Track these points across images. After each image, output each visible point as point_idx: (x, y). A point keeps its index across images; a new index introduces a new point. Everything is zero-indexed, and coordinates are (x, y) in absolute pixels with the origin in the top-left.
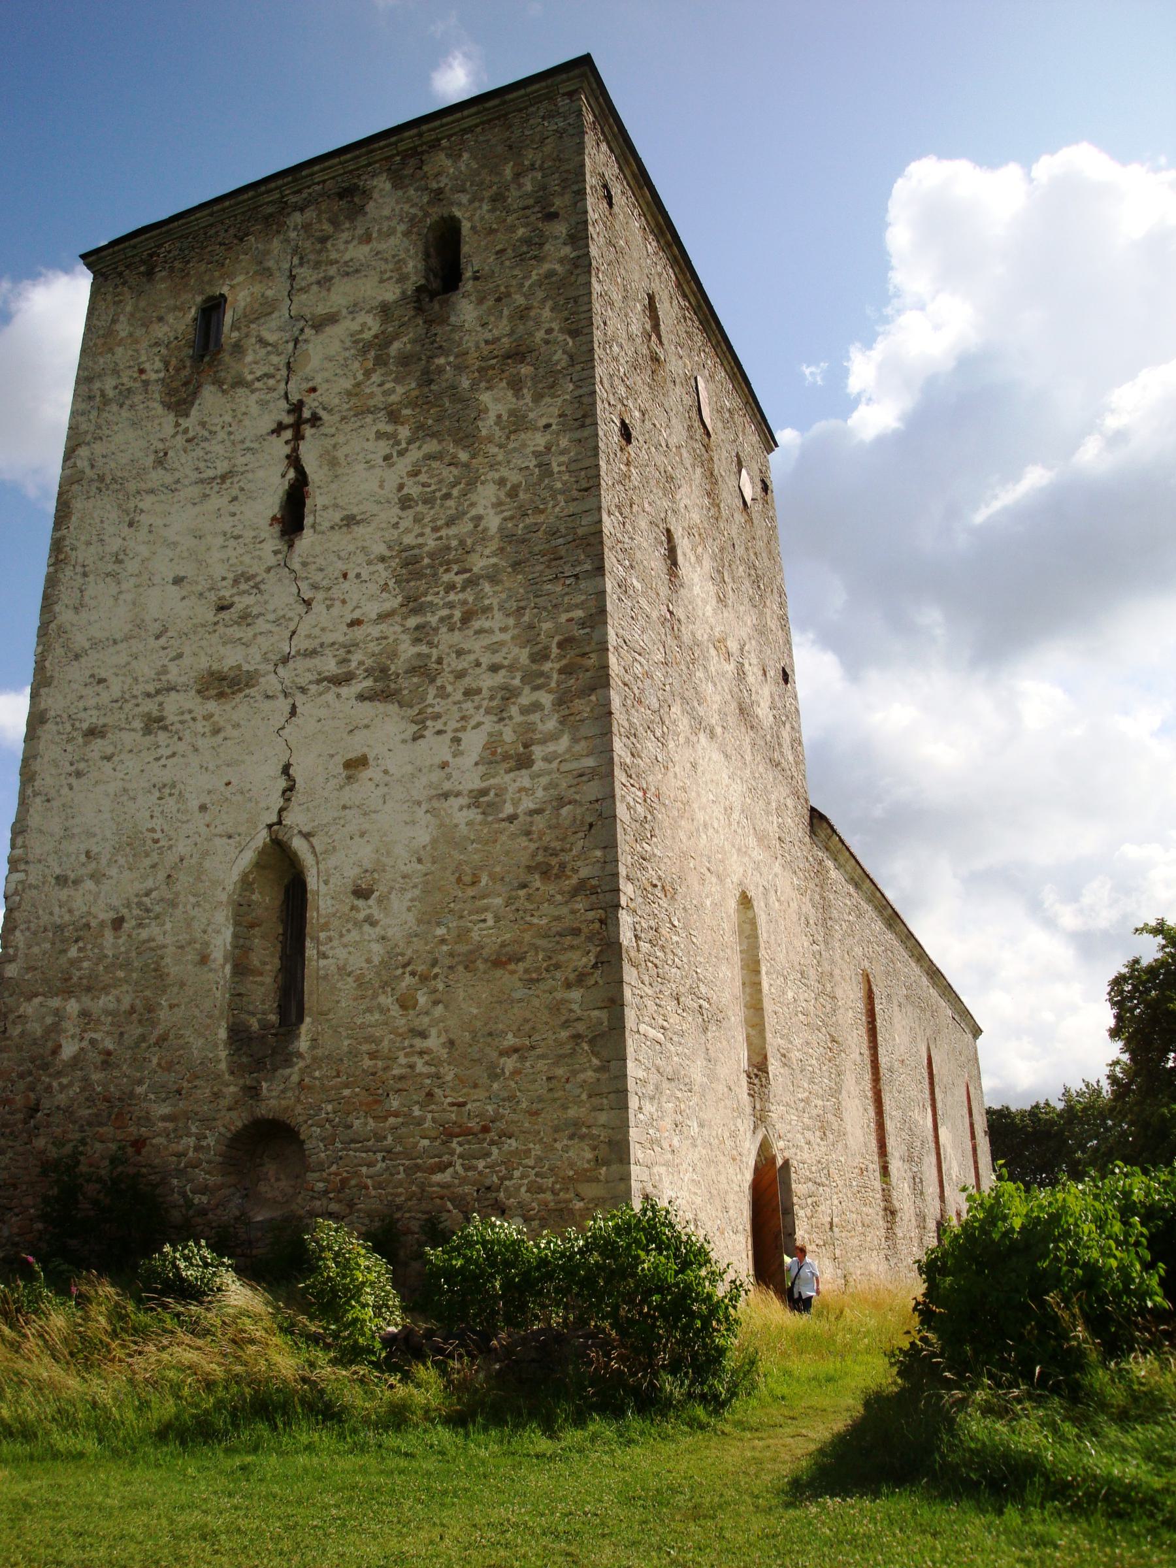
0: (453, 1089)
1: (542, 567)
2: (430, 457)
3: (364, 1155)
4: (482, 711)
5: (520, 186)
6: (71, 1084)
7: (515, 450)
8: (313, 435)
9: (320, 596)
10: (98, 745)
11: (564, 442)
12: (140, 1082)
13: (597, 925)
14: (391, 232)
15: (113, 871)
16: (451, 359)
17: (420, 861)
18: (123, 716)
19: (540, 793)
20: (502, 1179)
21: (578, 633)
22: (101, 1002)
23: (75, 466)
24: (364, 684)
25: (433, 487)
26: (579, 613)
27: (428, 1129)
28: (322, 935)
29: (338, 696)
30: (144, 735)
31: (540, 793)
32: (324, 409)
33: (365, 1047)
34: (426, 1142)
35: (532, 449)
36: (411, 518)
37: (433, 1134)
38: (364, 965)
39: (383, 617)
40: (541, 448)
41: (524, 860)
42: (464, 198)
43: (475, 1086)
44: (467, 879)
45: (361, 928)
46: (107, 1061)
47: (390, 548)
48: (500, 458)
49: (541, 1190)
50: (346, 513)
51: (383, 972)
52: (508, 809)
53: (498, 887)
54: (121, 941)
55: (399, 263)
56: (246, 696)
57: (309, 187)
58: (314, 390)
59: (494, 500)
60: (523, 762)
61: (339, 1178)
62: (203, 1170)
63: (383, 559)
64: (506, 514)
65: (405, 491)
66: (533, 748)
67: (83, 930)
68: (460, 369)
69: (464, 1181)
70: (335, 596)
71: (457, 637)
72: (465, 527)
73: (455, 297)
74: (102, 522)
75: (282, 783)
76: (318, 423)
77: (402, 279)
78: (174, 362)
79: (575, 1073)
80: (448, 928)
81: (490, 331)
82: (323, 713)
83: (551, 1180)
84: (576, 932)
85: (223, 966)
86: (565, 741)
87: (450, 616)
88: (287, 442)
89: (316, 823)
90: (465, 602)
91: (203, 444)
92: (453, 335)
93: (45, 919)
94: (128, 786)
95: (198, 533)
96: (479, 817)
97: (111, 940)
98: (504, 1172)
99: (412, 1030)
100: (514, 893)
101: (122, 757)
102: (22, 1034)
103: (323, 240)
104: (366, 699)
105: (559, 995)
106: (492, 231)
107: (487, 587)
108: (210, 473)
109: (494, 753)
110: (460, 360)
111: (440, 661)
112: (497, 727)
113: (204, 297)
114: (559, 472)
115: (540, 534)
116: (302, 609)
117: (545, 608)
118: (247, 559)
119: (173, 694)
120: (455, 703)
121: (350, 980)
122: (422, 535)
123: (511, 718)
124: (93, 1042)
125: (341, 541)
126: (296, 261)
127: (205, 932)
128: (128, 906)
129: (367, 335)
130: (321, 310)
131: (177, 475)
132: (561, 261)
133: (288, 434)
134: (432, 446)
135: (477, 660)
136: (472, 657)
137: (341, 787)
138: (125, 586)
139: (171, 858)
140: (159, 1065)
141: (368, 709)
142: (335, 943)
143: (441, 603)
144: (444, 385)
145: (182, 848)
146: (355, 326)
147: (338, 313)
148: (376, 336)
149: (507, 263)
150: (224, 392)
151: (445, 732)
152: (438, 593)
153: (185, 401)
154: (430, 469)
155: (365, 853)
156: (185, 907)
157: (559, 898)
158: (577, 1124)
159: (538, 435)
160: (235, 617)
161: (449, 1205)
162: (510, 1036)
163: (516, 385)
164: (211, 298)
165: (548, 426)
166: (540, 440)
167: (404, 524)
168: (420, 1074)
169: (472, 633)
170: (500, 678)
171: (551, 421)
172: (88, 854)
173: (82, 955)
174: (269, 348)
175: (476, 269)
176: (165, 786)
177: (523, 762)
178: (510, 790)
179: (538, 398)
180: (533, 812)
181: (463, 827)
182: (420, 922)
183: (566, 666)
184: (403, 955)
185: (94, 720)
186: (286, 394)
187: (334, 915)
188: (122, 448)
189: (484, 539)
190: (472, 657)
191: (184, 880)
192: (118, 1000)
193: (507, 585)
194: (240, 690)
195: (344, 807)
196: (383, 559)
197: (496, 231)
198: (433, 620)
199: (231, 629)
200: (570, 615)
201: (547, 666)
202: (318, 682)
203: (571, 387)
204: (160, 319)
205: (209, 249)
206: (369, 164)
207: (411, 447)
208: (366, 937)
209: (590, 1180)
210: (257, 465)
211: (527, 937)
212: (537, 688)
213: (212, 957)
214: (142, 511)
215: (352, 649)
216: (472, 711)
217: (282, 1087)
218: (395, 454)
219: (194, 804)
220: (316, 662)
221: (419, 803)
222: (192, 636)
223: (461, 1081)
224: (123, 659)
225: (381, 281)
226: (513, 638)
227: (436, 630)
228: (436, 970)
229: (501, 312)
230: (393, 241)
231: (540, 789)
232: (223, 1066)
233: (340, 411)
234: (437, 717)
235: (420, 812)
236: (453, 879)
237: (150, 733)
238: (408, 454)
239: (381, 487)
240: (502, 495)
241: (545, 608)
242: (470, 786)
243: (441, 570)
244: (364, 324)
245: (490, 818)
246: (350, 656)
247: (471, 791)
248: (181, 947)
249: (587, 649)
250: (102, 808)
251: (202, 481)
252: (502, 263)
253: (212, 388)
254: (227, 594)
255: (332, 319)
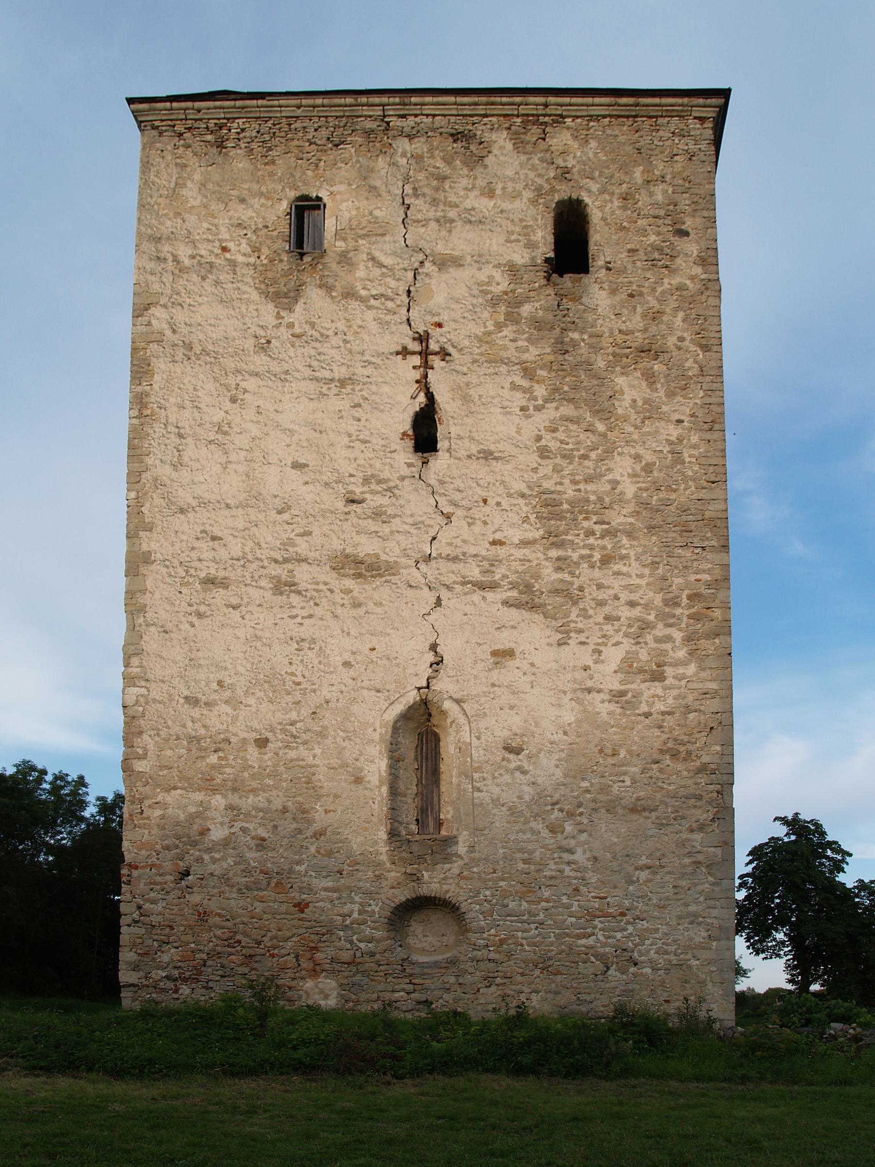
1: (674, 535)
3: (520, 925)
4: (621, 633)
5: (651, 194)
6: (224, 858)
7: (649, 433)
8: (442, 368)
9: (460, 513)
10: (219, 596)
11: (695, 439)
12: (299, 863)
13: (715, 795)
14: (516, 196)
15: (252, 701)
16: (586, 337)
17: (565, 733)
18: (247, 574)
19: (670, 701)
20: (636, 945)
21: (704, 591)
22: (250, 801)
23: (149, 324)
25: (571, 446)
26: (706, 577)
27: (575, 911)
29: (484, 598)
30: (274, 594)
31: (670, 701)
32: (454, 347)
34: (573, 919)
35: (665, 437)
36: (551, 468)
37: (579, 915)
38: (516, 800)
39: (525, 543)
40: (673, 438)
41: (657, 745)
42: (595, 187)
43: (615, 887)
44: (609, 752)
45: (512, 773)
46: (261, 844)
47: (529, 487)
48: (635, 437)
49: (666, 953)
50: (482, 447)
52: (644, 708)
53: (635, 760)
54: (266, 757)
55: (527, 231)
56: (386, 581)
57: (416, 116)
58: (440, 325)
59: (630, 471)
61: (497, 938)
62: (368, 926)
63: (523, 496)
64: (640, 485)
65: (543, 442)
66: (665, 668)
67: (221, 744)
68: (595, 348)
69: (605, 945)
70: (477, 516)
71: (597, 573)
72: (603, 487)
73: (586, 279)
74: (195, 389)
75: (431, 657)
76: (448, 358)
77: (531, 245)
78: (265, 251)
79: (696, 885)
80: (592, 784)
81: (624, 322)
82: (469, 609)
83: (674, 947)
84: (699, 798)
85: (380, 787)
86: (691, 669)
87: (591, 556)
88: (414, 367)
89: (465, 693)
90: (604, 548)
91: (314, 344)
92: (585, 315)
93: (176, 729)
94: (259, 633)
95: (317, 428)
96: (619, 711)
97: (256, 754)
98: (638, 940)
99: (560, 848)
100: (648, 766)
101: (249, 608)
102: (162, 817)
103: (442, 178)
104: (511, 606)
106: (622, 228)
107: (625, 541)
108: (327, 374)
109: (631, 666)
110: (594, 340)
111: (581, 589)
112: (634, 648)
113: (298, 194)
114: (690, 462)
115: (673, 508)
116: (442, 520)
117: (676, 567)
118: (378, 464)
119: (304, 566)
120: (596, 624)
121: (504, 809)
122: (561, 484)
123: (646, 643)
124: (244, 830)
125: (480, 470)
126: (408, 189)
127: (357, 760)
128: (272, 730)
129: (497, 290)
130: (440, 248)
131: (286, 367)
132: (692, 278)
134: (568, 410)
136: (611, 592)
137: (490, 670)
138: (233, 457)
139: (314, 700)
140: (318, 852)
141: (514, 615)
142: (489, 782)
143: (582, 544)
144: (579, 359)
145: (325, 693)
146: (482, 276)
147: (461, 258)
148: (506, 293)
149: (639, 264)
150: (332, 297)
151: (588, 644)
152: (578, 535)
153: (286, 295)
154: (567, 430)
155: (516, 722)
156: (335, 738)
157: (685, 773)
158: (696, 915)
159: (671, 427)
160: (369, 512)
161: (593, 959)
163: (650, 378)
164: (305, 198)
165: (680, 421)
166: (674, 432)
167: (542, 472)
168: (569, 877)
169: (611, 573)
170: (637, 612)
171: (682, 418)
172: (220, 683)
173: (223, 763)
174: (384, 270)
175: (608, 259)
176: (303, 640)
177: (657, 677)
178: (645, 695)
179: (671, 394)
180: (663, 713)
182: (566, 776)
183: (695, 614)
184: (551, 797)
185: (213, 572)
186: (408, 320)
187: (487, 762)
188: (212, 321)
189: (621, 500)
190: (611, 592)
191: (329, 719)
192: (269, 802)
193: (642, 542)
194: (381, 576)
195: (493, 685)
196: (523, 496)
197: (628, 229)
198: (575, 556)
199: (366, 522)
200: (699, 577)
201: (678, 611)
202: (463, 584)
203: (701, 394)
204: (243, 201)
205: (295, 143)
206: (486, 116)
207: (547, 405)
208: (518, 781)
210: (380, 380)
211: (659, 796)
212: (671, 625)
213: (367, 779)
214: (245, 391)
215: (496, 563)
216: (611, 632)
217: (442, 876)
218: (531, 408)
219: (337, 660)
220: (460, 566)
221: (565, 693)
222: (321, 519)
223: (603, 883)
224: (241, 523)
226: (648, 584)
227: (577, 564)
228: (581, 810)
229: (635, 308)
230: (517, 204)
231: (671, 698)
232: (384, 858)
233: (471, 354)
234: (581, 631)
235: (566, 699)
236: (596, 750)
237: (281, 594)
238: (543, 411)
239: (518, 432)
240: (638, 468)
241: (676, 567)
242: (611, 687)
243: (581, 517)
244: (491, 277)
245: (628, 712)
246: (494, 569)
247: (611, 691)
248: (334, 768)
249: (713, 605)
250: (232, 648)
251: (317, 380)
252: (634, 262)
253: (321, 292)
254: (358, 490)
255: (457, 262)
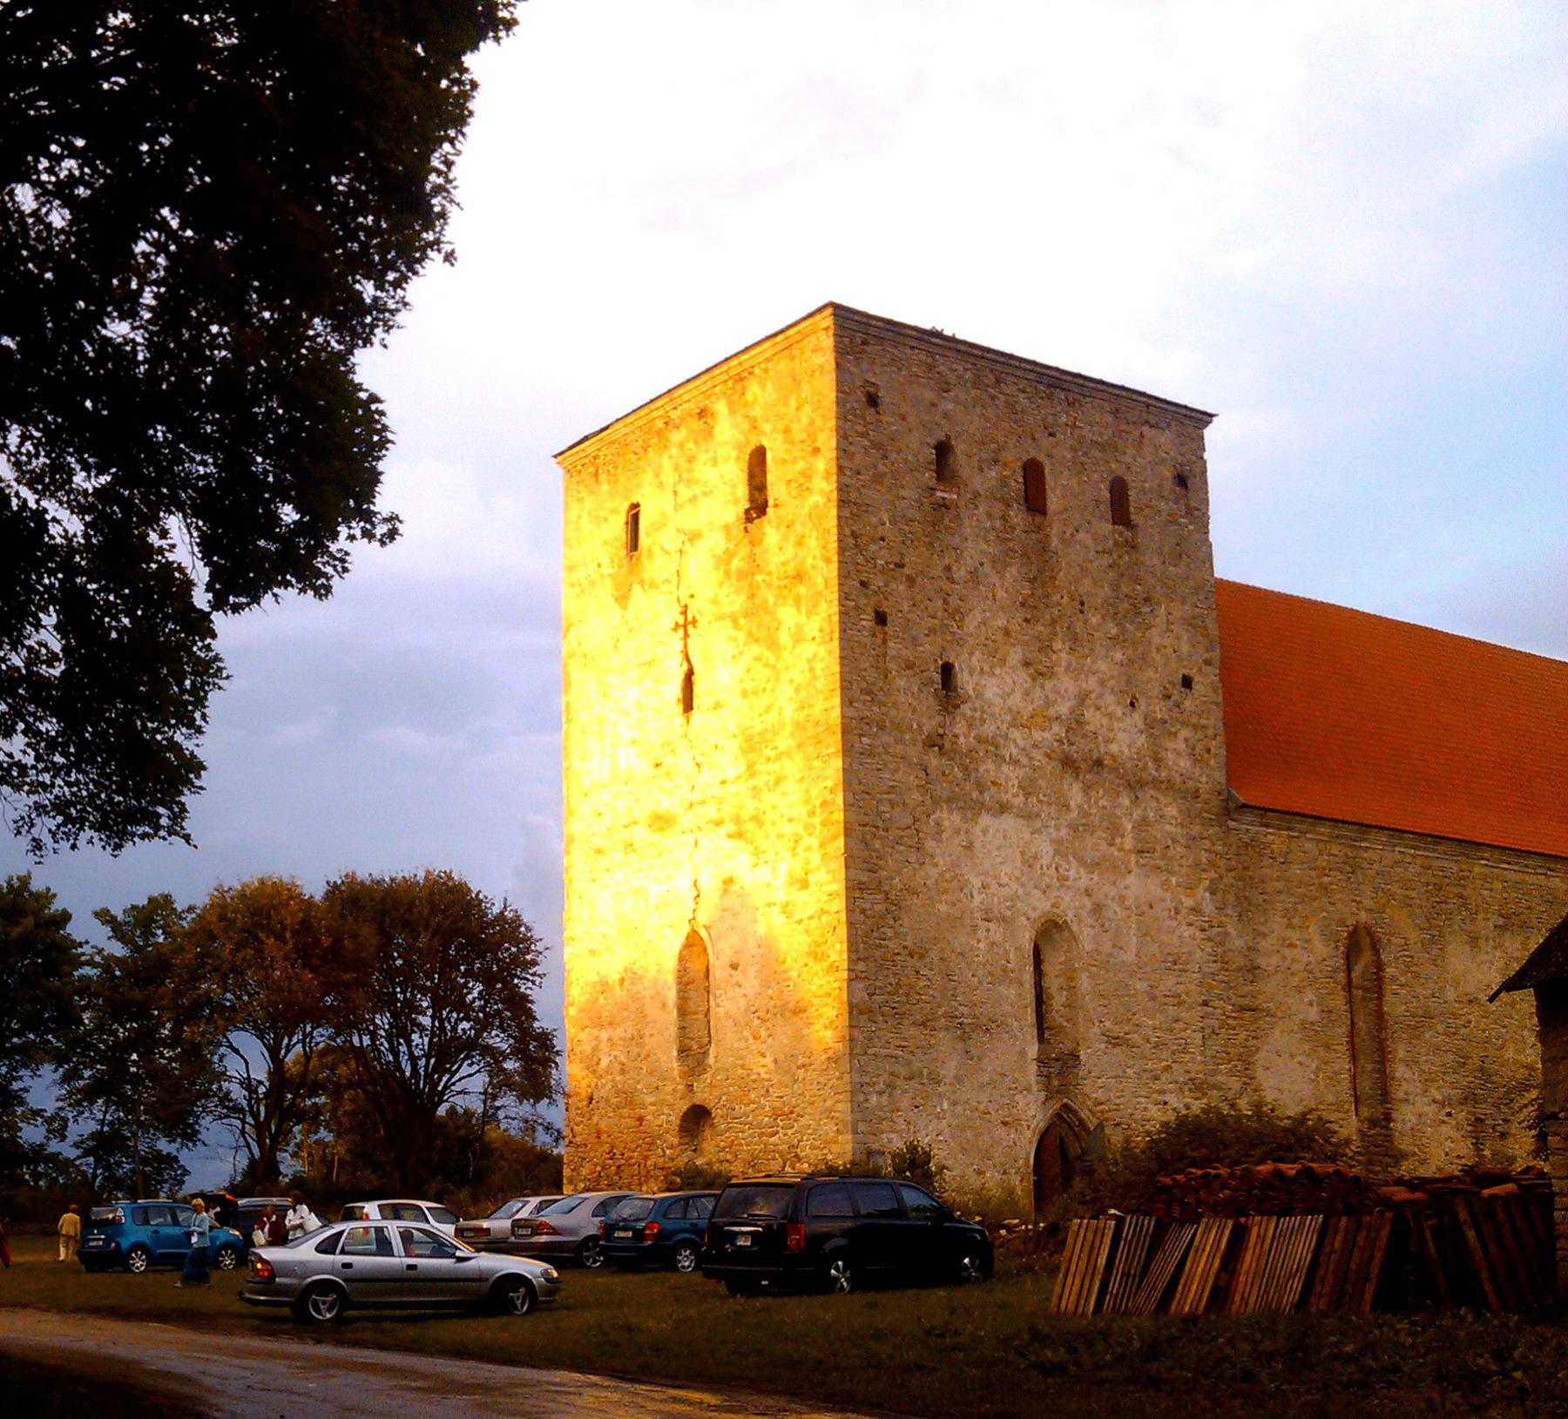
5: (799, 420)
24: (730, 827)
41: (805, 948)
60: (804, 884)
75: (695, 894)
133: (681, 631)
163: (797, 602)
165: (814, 639)
179: (809, 614)
209: (835, 1142)
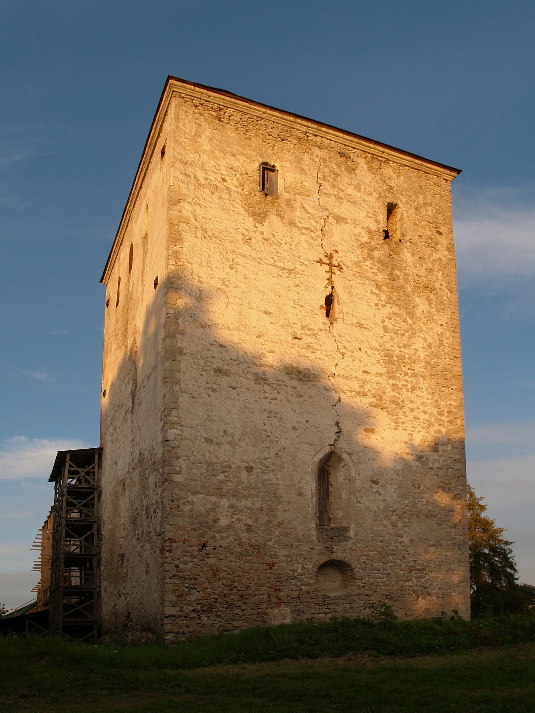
0: (412, 556)
2: (396, 314)
4: (420, 426)
17: (398, 475)
20: (430, 585)
28: (358, 495)
31: (441, 462)
33: (378, 538)
38: (376, 508)
44: (416, 486)
45: (375, 495)
49: (442, 589)
51: (384, 512)
52: (430, 465)
65: (385, 324)
66: (439, 446)
71: (409, 394)
83: (445, 586)
87: (407, 386)
96: (420, 465)
99: (397, 534)
105: (449, 530)
122: (393, 347)
134: (395, 309)
135: (418, 406)
136: (416, 405)
143: (403, 379)
152: (401, 374)
162: (432, 540)
168: (400, 550)
170: (426, 416)
180: (438, 468)
181: (414, 467)
182: (398, 497)
190: (416, 405)
198: (400, 385)
208: (377, 498)
211: (437, 509)
225: (367, 216)
227: (401, 389)
228: (405, 515)
234: (403, 423)
245: (424, 467)
247: (417, 455)
